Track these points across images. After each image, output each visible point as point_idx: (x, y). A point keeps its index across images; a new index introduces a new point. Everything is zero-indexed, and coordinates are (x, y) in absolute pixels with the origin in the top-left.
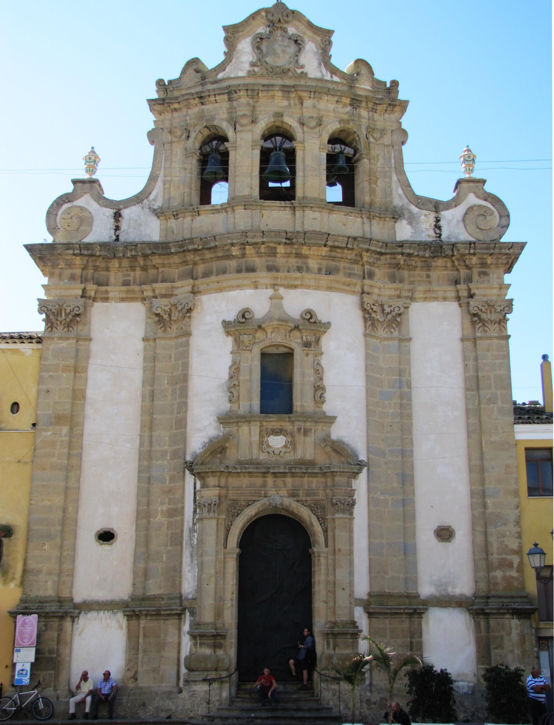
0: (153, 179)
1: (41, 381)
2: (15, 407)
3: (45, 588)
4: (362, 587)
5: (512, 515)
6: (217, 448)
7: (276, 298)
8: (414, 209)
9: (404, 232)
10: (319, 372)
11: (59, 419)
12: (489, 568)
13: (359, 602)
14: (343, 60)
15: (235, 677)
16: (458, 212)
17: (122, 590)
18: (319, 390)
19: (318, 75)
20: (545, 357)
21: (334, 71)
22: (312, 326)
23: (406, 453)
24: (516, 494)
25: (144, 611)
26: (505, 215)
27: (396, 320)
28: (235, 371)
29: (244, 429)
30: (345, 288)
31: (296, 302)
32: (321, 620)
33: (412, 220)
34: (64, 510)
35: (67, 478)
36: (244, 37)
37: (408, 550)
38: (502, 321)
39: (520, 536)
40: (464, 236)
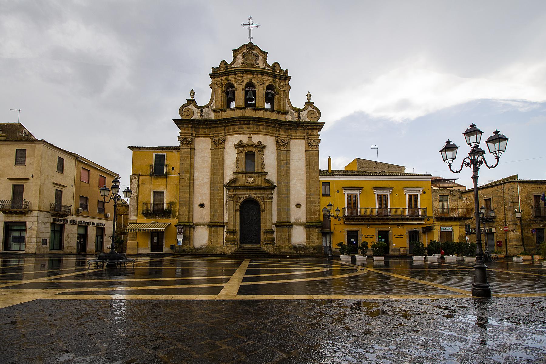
0: (212, 100)
1: (181, 161)
2: (173, 169)
3: (185, 219)
4: (275, 220)
5: (317, 201)
6: (233, 181)
7: (250, 138)
8: (292, 111)
9: (289, 118)
10: (263, 159)
11: (186, 172)
12: (311, 215)
13: (274, 224)
14: (270, 62)
15: (239, 243)
16: (306, 112)
17: (207, 220)
18: (263, 164)
19: (263, 67)
20: (329, 157)
21: (268, 66)
22: (261, 147)
23: (288, 183)
24: (319, 195)
25: (214, 226)
26: (319, 113)
27: (287, 144)
28: (238, 158)
29: (241, 176)
30: (271, 134)
31: (256, 139)
32: (263, 228)
33: (292, 114)
34: (189, 198)
35: (190, 189)
36: (239, 53)
37: (288, 210)
38: (317, 146)
39: (319, 206)
40: (307, 120)
